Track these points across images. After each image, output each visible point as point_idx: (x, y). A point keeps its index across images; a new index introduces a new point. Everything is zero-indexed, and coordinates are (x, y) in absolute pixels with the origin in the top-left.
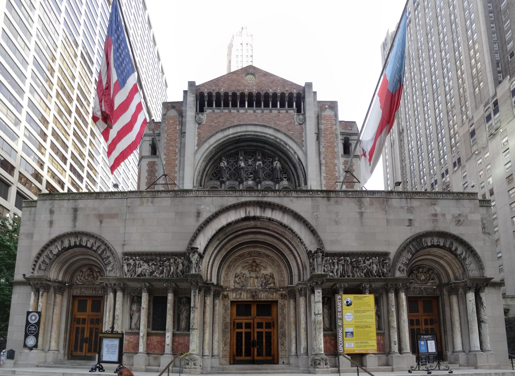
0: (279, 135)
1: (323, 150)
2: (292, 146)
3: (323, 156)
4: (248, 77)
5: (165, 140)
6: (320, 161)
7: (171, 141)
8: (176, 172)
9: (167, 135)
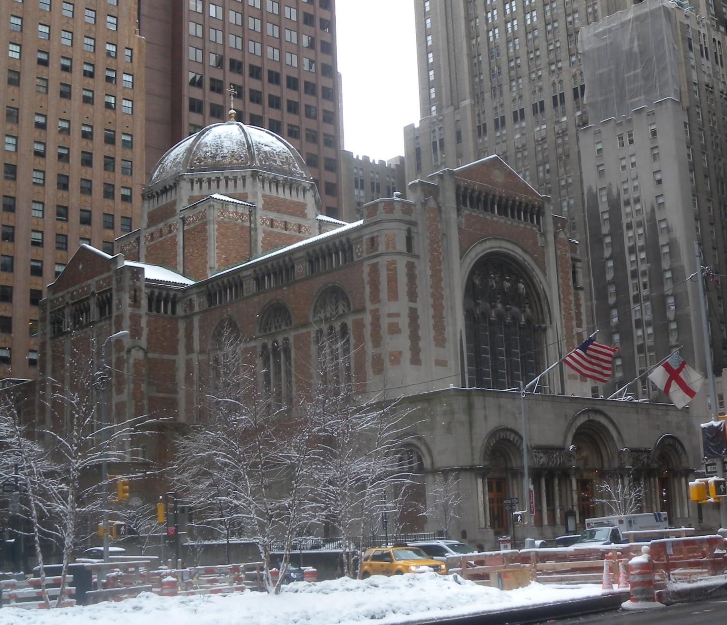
2: (537, 271)
3: (561, 289)
5: (429, 241)
6: (559, 295)
9: (430, 233)
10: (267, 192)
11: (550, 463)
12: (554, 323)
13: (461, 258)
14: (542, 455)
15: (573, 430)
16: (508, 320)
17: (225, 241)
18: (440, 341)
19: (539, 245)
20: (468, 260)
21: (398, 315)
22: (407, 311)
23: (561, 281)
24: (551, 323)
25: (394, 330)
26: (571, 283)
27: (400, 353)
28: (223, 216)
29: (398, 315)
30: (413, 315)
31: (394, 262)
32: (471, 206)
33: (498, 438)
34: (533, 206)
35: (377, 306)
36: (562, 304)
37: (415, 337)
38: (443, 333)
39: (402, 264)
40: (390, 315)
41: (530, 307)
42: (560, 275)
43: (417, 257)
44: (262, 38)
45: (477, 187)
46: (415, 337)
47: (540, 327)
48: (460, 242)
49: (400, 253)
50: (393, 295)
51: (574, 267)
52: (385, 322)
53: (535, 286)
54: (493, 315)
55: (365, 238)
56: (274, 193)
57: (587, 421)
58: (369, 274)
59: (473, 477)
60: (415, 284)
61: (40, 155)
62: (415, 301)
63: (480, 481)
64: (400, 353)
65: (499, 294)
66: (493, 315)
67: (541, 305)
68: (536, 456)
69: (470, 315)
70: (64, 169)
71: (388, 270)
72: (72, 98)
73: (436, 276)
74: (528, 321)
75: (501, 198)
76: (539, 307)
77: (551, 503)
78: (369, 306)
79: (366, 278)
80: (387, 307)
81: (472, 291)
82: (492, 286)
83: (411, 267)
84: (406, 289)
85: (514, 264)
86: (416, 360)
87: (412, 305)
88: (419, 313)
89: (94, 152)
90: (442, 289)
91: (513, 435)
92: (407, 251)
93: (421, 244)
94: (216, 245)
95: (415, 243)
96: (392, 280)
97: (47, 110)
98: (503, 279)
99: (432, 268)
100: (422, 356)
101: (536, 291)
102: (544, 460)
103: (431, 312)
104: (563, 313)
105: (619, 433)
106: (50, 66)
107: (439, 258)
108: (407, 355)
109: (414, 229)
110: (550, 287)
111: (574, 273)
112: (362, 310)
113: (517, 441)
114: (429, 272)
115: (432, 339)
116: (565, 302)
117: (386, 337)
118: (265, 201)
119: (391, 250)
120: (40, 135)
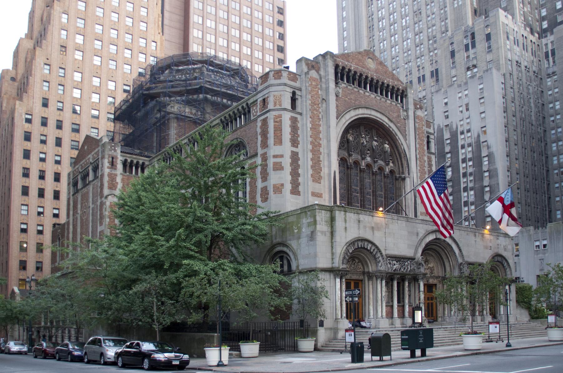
0: (392, 125)
1: (418, 146)
2: (399, 136)
3: (418, 151)
5: (310, 102)
6: (416, 155)
9: (312, 97)
11: (402, 270)
12: (411, 175)
13: (337, 118)
14: (395, 262)
15: (423, 245)
16: (375, 169)
18: (317, 178)
20: (343, 120)
21: (282, 156)
22: (290, 154)
23: (418, 146)
24: (409, 174)
25: (278, 167)
26: (426, 148)
27: (282, 185)
29: (282, 156)
30: (295, 157)
31: (280, 116)
33: (356, 246)
35: (265, 150)
36: (418, 162)
37: (295, 174)
38: (320, 173)
39: (286, 117)
40: (275, 156)
41: (393, 162)
42: (418, 141)
44: (240, 41)
46: (295, 174)
47: (400, 177)
48: (337, 106)
49: (285, 109)
50: (279, 141)
51: (428, 137)
52: (271, 162)
53: (397, 147)
54: (363, 164)
55: (259, 100)
57: (435, 239)
58: (261, 128)
59: (332, 276)
60: (297, 134)
62: (297, 147)
63: (338, 280)
64: (282, 185)
65: (368, 150)
66: (363, 164)
67: (401, 161)
68: (390, 263)
69: (343, 161)
71: (275, 122)
73: (315, 129)
74: (392, 172)
76: (400, 163)
77: (401, 300)
78: (260, 151)
79: (259, 130)
80: (274, 150)
81: (344, 144)
82: (363, 143)
83: (294, 121)
84: (290, 137)
85: (381, 130)
86: (295, 191)
87: (294, 149)
88: (300, 156)
90: (320, 139)
91: (370, 245)
92: (292, 108)
93: (303, 104)
94: (175, 132)
95: (298, 103)
96: (278, 129)
98: (372, 139)
99: (312, 123)
100: (301, 188)
101: (398, 150)
102: (397, 266)
103: (310, 155)
104: (419, 168)
105: (460, 250)
107: (319, 116)
108: (288, 187)
109: (298, 92)
110: (409, 149)
111: (428, 142)
112: (256, 155)
113: (374, 250)
114: (309, 125)
115: (310, 176)
116: (420, 161)
119: (278, 107)
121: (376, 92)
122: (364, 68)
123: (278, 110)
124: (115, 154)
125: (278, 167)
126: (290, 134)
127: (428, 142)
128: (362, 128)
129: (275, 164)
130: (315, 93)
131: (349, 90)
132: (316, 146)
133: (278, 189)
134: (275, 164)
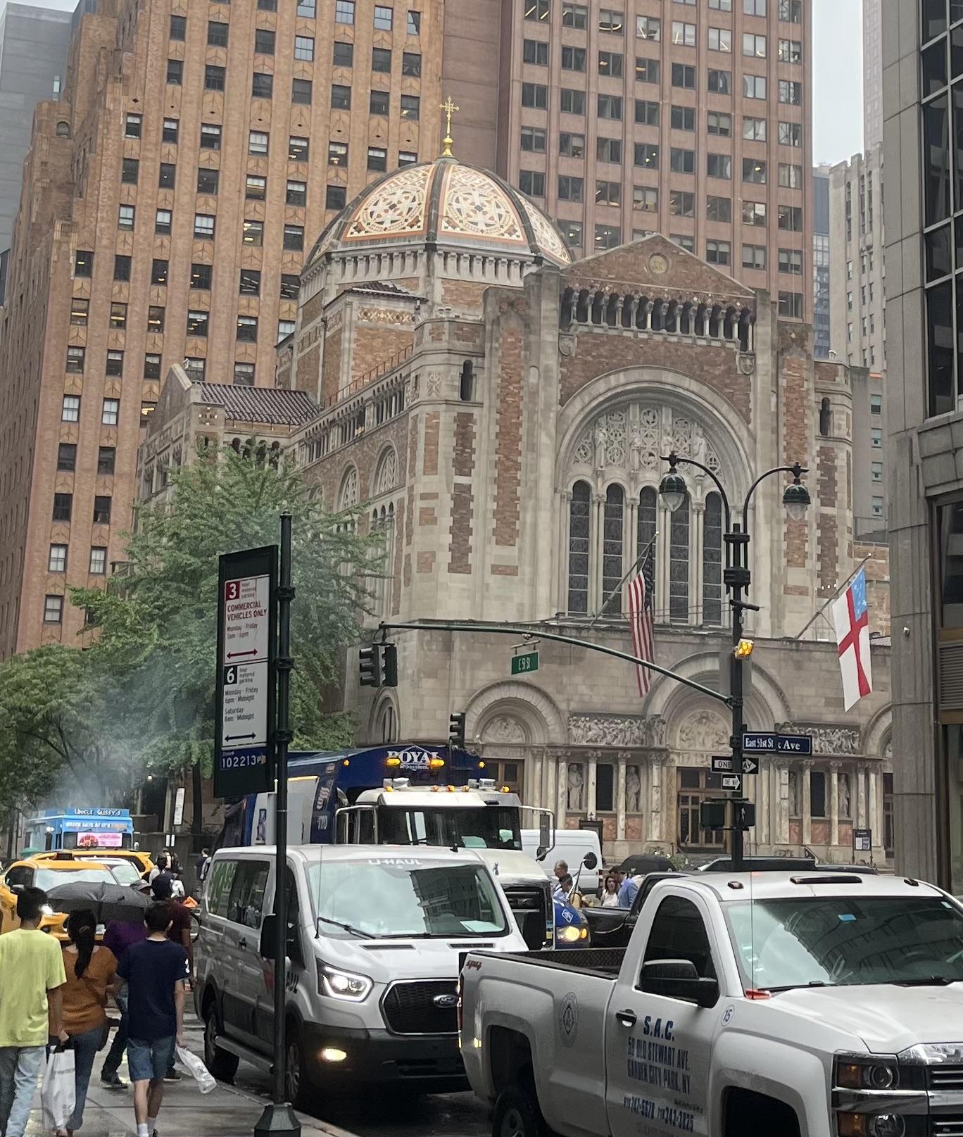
4: (655, 258)
5: (499, 381)
7: (510, 384)
8: (520, 453)
9: (503, 369)
10: (451, 273)
17: (369, 358)
19: (739, 372)
27: (433, 554)
28: (368, 319)
29: (434, 496)
30: (462, 498)
31: (436, 416)
32: (596, 320)
34: (731, 311)
37: (461, 530)
38: (514, 523)
39: (446, 419)
40: (424, 497)
43: (481, 405)
45: (607, 289)
46: (461, 530)
50: (431, 468)
52: (419, 504)
56: (465, 275)
60: (471, 448)
61: (256, 196)
62: (469, 475)
65: (651, 454)
70: (296, 215)
71: (427, 427)
72: (313, 102)
75: (659, 302)
80: (424, 483)
83: (464, 422)
86: (459, 563)
87: (463, 480)
89: (348, 186)
92: (462, 397)
94: (352, 363)
96: (432, 441)
97: (270, 124)
106: (276, 54)
108: (445, 557)
117: (417, 528)
118: (447, 290)
120: (257, 165)
121: (671, 329)
122: (639, 281)
123: (432, 402)
124: (213, 430)
125: (429, 518)
126: (454, 450)
127: (825, 414)
128: (634, 412)
129: (423, 511)
130: (511, 359)
131: (597, 336)
132: (507, 469)
133: (427, 562)
134: (423, 511)
